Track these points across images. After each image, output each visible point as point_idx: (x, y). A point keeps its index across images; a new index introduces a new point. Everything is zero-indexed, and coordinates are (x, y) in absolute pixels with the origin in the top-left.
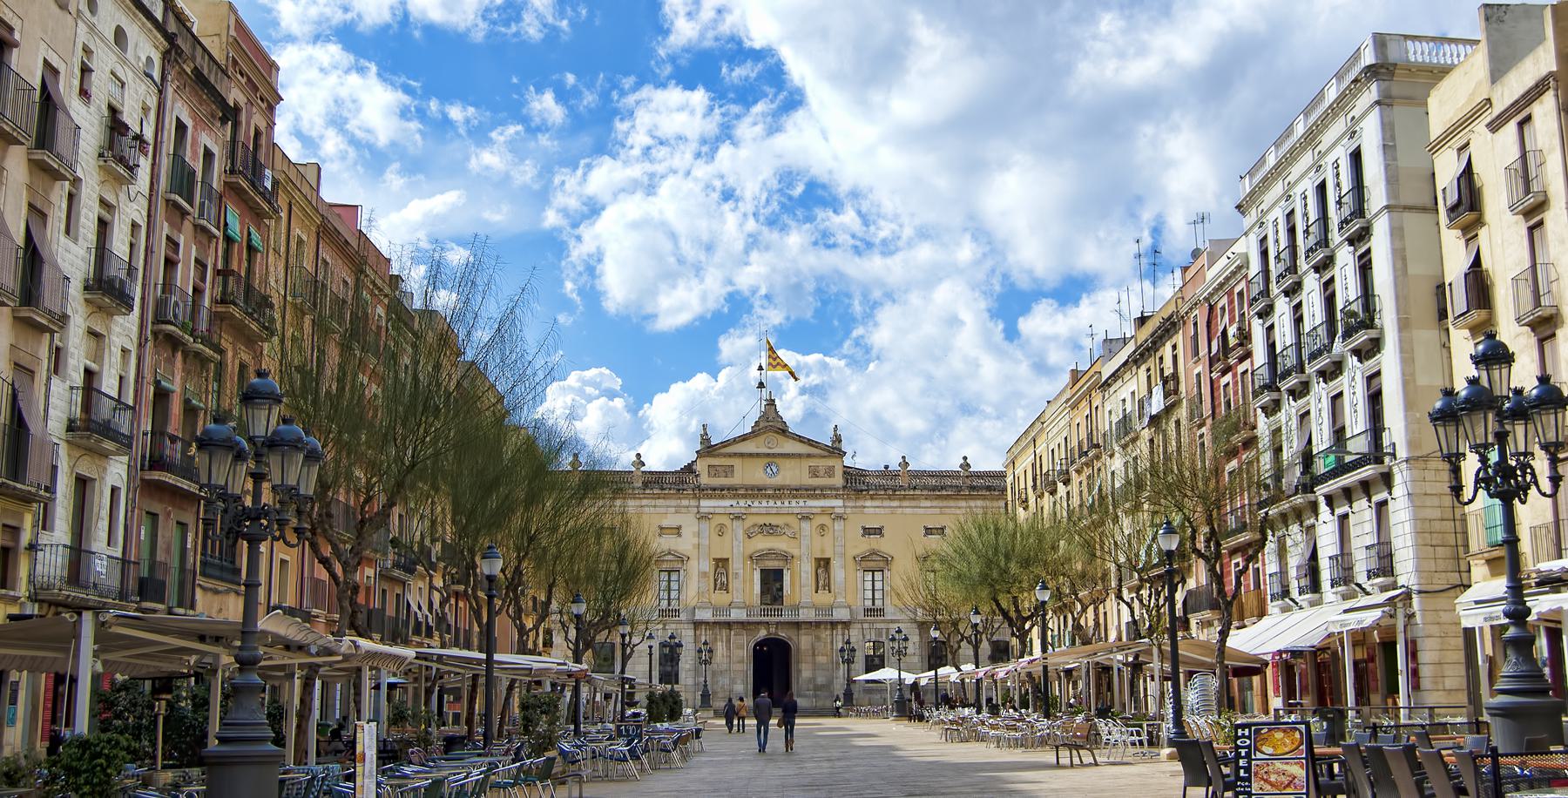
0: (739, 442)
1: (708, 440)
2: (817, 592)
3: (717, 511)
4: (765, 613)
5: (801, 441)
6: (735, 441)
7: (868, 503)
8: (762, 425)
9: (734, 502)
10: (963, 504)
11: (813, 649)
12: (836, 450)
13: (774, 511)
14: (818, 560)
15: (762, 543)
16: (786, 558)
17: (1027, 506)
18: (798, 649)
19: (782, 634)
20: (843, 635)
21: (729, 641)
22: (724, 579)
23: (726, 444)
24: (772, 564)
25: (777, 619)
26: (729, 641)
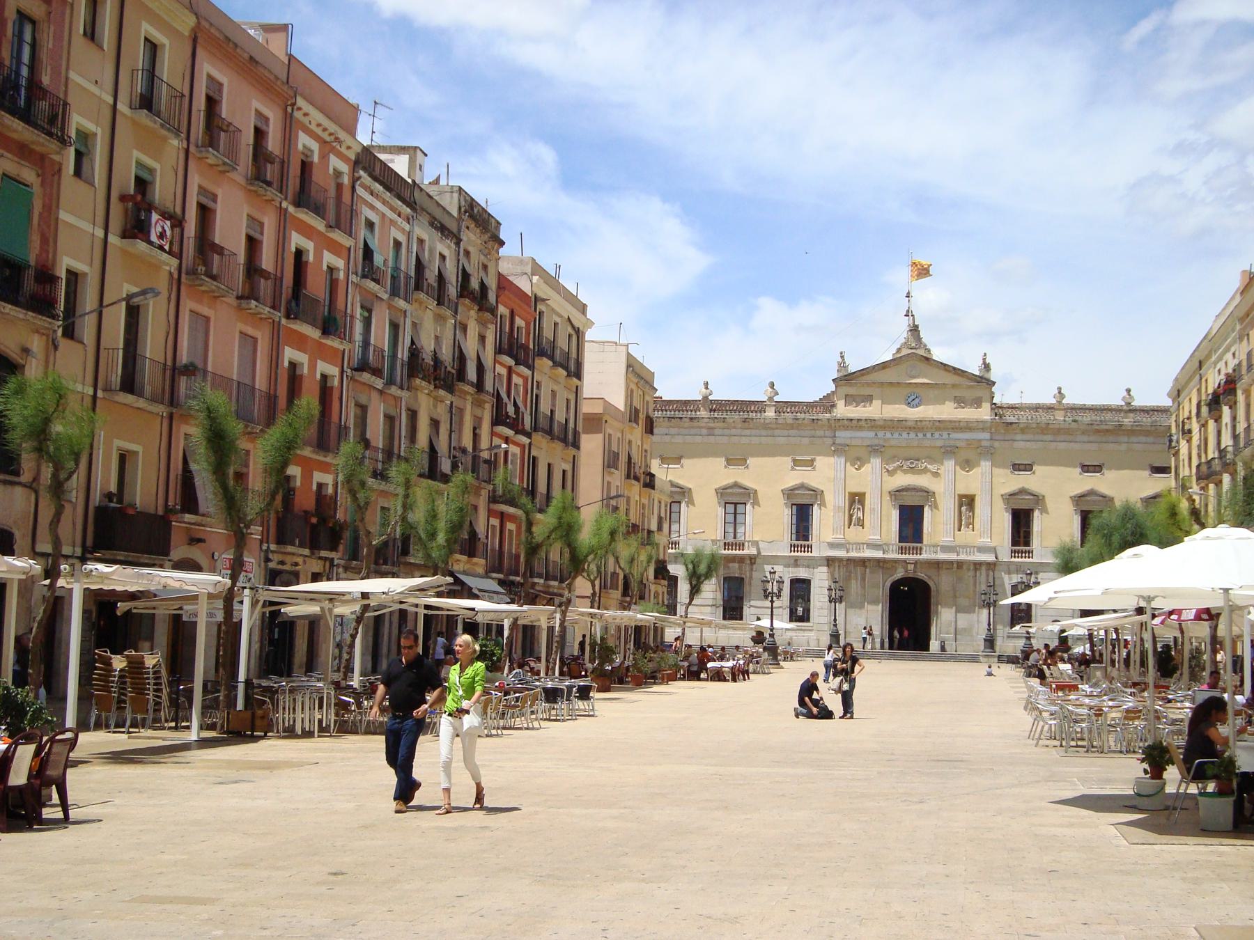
0: (879, 370)
1: (846, 368)
2: (959, 530)
3: (854, 442)
4: (902, 550)
5: (946, 370)
6: (874, 368)
7: (1019, 437)
8: (905, 352)
9: (871, 434)
10: (1125, 439)
11: (954, 590)
12: (983, 382)
13: (915, 444)
14: (961, 497)
15: (902, 480)
16: (928, 494)
17: (1191, 438)
18: (937, 591)
19: (921, 575)
20: (988, 576)
21: (863, 579)
22: (860, 514)
23: (864, 372)
24: (911, 500)
25: (915, 557)
26: (863, 579)
